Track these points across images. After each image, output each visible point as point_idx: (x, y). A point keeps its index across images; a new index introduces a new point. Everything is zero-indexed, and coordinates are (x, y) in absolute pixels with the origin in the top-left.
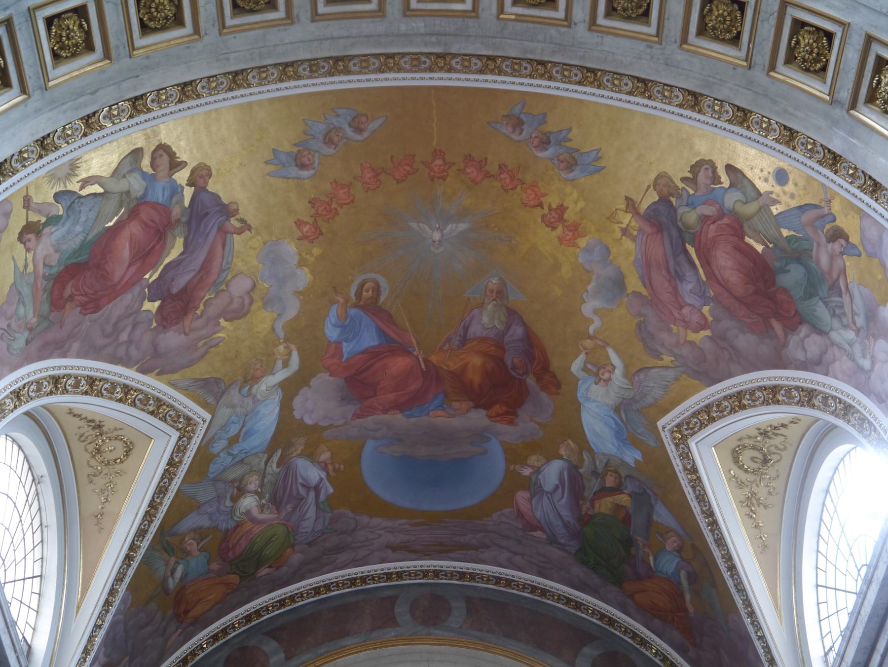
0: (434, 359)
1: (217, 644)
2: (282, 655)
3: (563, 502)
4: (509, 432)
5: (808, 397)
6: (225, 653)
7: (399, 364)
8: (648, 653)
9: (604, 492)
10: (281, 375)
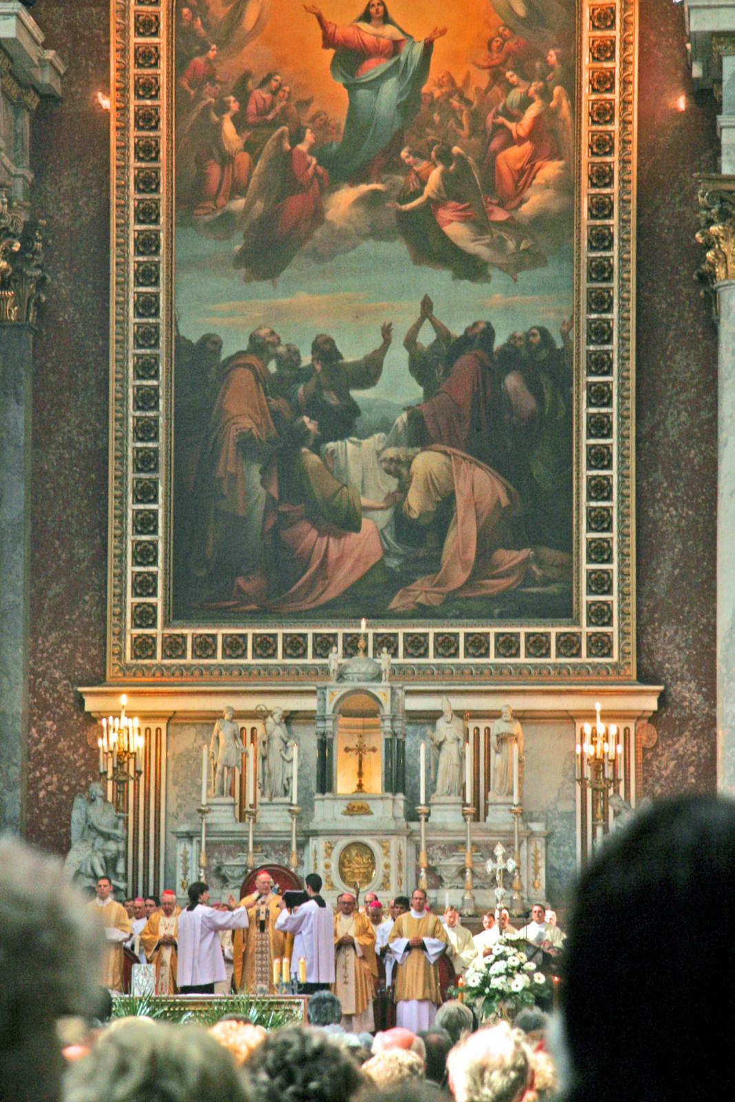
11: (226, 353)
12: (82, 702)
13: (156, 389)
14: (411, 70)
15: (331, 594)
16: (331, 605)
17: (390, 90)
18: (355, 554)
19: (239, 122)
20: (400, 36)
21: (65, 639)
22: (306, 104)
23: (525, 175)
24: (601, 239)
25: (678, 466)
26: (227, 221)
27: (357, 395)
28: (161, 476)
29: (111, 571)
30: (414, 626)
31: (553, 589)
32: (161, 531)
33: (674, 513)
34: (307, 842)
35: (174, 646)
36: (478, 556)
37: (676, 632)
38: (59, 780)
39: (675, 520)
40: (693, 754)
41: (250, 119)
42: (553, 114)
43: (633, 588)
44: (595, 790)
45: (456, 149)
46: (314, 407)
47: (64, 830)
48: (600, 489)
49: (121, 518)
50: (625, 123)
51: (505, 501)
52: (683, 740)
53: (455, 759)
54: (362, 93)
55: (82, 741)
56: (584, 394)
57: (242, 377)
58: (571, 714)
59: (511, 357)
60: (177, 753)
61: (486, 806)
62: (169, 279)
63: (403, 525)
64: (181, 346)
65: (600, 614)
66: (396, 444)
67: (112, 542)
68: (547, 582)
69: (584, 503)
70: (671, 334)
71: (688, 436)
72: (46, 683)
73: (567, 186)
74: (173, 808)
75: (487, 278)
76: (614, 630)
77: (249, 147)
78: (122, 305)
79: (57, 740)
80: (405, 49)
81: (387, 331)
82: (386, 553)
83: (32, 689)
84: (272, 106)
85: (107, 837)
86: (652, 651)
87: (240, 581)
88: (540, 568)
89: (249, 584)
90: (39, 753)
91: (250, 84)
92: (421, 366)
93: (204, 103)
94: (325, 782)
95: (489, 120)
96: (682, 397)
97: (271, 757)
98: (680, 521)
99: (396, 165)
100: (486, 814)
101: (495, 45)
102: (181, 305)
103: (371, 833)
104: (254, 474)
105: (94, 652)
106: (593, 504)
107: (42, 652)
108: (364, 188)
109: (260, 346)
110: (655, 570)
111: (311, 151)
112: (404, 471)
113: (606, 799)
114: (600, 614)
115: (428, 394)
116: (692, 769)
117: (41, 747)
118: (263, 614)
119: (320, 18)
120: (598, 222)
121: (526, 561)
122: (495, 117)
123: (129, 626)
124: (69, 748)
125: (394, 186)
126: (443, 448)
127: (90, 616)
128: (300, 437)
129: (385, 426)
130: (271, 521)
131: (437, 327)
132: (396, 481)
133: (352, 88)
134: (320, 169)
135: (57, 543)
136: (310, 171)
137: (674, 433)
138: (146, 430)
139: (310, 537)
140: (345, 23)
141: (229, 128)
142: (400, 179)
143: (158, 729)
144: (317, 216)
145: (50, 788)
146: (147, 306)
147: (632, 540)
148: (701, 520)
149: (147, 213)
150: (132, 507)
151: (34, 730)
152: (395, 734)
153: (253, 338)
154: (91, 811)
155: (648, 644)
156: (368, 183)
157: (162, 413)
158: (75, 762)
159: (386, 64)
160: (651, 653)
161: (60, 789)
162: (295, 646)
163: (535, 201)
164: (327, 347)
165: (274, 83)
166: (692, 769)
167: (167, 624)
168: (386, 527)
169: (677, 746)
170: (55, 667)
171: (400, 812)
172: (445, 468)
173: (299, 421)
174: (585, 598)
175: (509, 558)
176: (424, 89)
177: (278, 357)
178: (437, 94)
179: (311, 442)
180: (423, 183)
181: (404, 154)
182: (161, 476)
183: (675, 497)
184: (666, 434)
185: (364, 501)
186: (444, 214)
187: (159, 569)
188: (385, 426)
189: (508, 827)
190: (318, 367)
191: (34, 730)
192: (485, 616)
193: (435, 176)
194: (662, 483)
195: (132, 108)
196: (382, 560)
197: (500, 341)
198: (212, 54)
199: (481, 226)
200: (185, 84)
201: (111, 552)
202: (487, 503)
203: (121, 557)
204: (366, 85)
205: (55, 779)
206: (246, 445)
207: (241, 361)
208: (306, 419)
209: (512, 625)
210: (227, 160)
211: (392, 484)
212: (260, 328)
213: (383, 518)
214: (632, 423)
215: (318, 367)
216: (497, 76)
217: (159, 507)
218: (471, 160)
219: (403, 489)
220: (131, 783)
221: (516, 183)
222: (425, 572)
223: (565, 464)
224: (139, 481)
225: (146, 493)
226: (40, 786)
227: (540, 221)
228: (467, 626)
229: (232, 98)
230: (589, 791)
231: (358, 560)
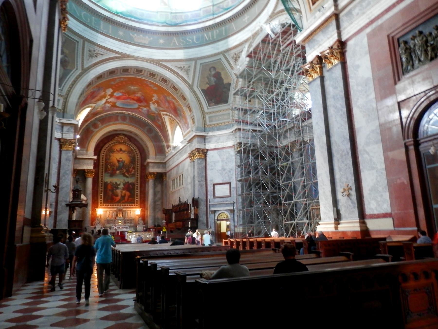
0: (130, 97)
3: (146, 112)
4: (140, 104)
5: (178, 123)
7: (124, 97)
9: (152, 113)
10: (106, 98)
26: (108, 173)
27: (119, 186)
46: (115, 187)
57: (109, 185)
63: (122, 196)
65: (137, 203)
69: (136, 195)
73: (135, 172)
77: (111, 168)
81: (121, 182)
92: (124, 184)
109: (111, 182)
111: (116, 168)
114: (137, 203)
118: (111, 203)
129: (120, 189)
138: (102, 189)
140: (118, 159)
141: (109, 166)
144: (115, 173)
149: (102, 172)
157: (103, 187)
163: (133, 173)
175: (130, 199)
193: (125, 171)
199: (128, 174)
206: (110, 190)
210: (109, 168)
211: (121, 193)
217: (102, 195)
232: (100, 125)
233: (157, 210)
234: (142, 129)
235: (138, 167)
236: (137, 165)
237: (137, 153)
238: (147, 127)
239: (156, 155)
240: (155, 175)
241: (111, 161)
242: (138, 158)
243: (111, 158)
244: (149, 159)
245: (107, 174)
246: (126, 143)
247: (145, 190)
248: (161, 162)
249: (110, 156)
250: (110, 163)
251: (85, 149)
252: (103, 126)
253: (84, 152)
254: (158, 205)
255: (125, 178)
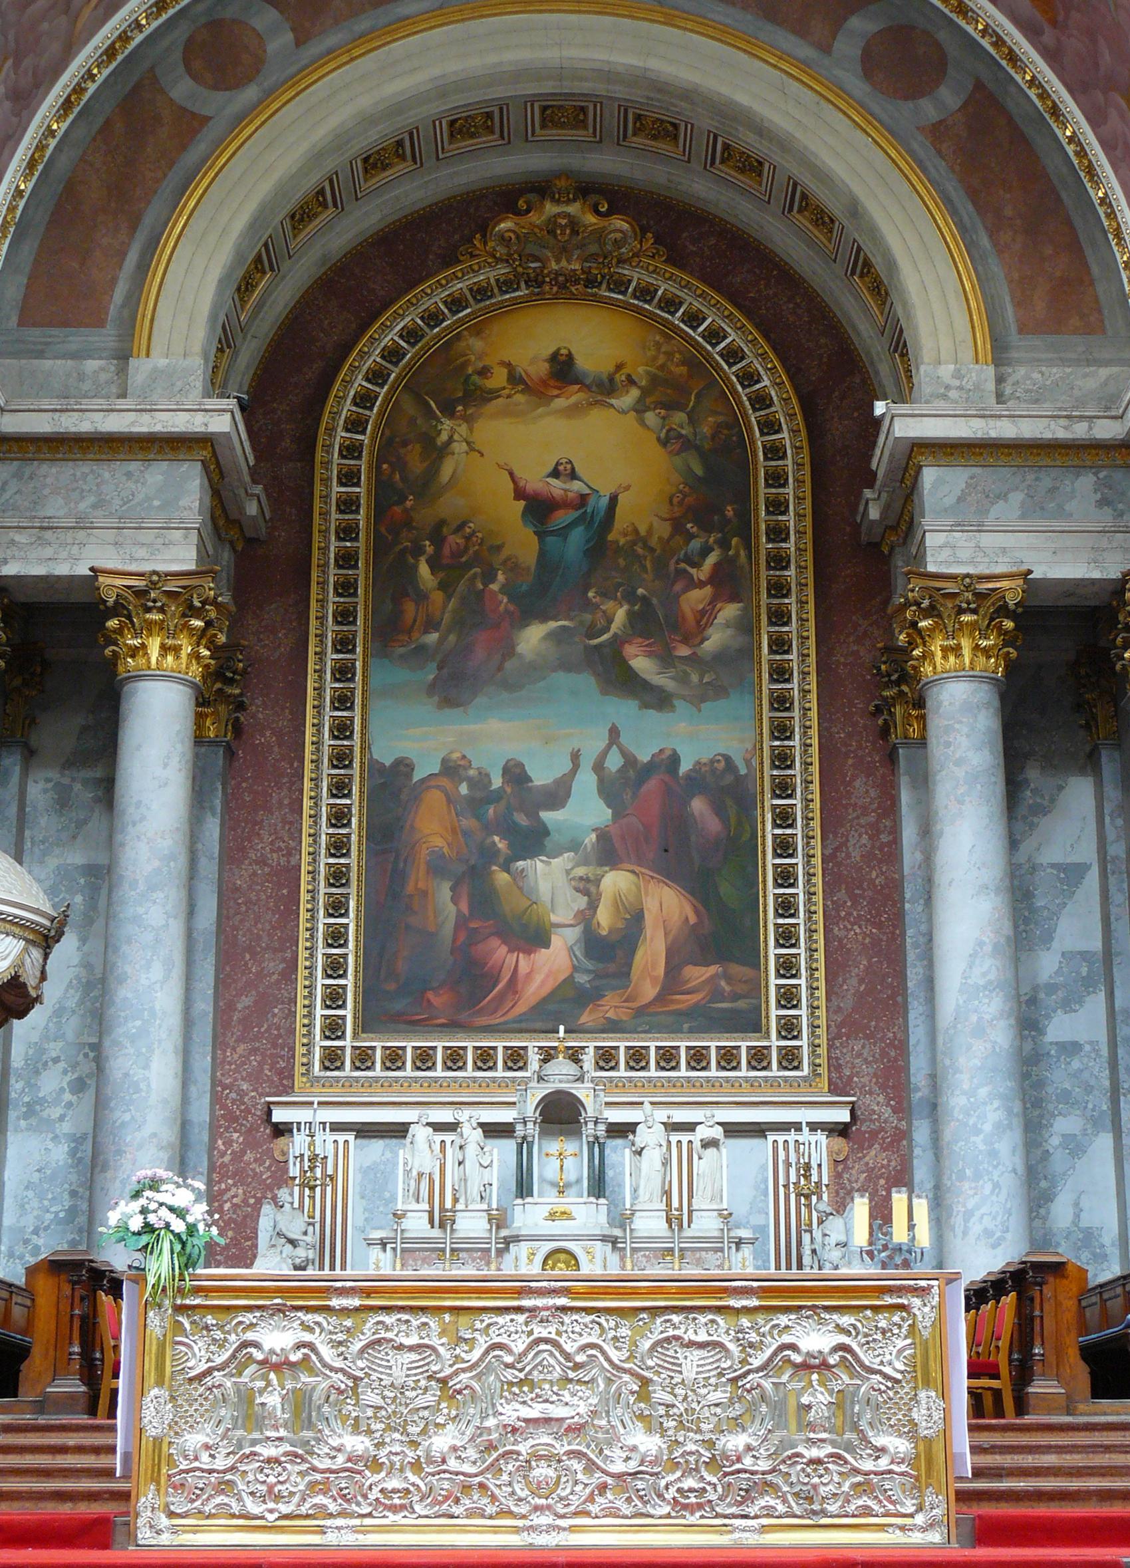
1: (165, 17)
2: (290, 36)
6: (181, 34)
8: (970, 29)
11: (418, 776)
12: (269, 1113)
13: (349, 807)
14: (597, 520)
15: (522, 1008)
16: (520, 1019)
17: (577, 536)
18: (545, 970)
19: (434, 565)
20: (588, 491)
21: (254, 1051)
22: (499, 548)
23: (705, 617)
24: (780, 673)
25: (860, 887)
27: (546, 816)
28: (353, 890)
29: (301, 982)
30: (604, 1040)
31: (741, 1004)
32: (351, 944)
33: (858, 931)
34: (507, 1249)
35: (363, 1058)
36: (667, 973)
37: (863, 1047)
38: (244, 1193)
39: (860, 937)
40: (883, 1166)
41: (445, 561)
42: (732, 561)
43: (823, 1003)
44: (798, 1195)
45: (640, 591)
47: (249, 1243)
48: (786, 907)
49: (312, 930)
50: (801, 569)
51: (693, 919)
52: (873, 1153)
53: (658, 1165)
54: (550, 539)
55: (269, 1153)
56: (769, 816)
57: (435, 798)
58: (764, 1127)
59: (698, 781)
60: (365, 1165)
61: (690, 1212)
62: (364, 706)
64: (374, 769)
66: (585, 862)
67: (302, 954)
68: (735, 997)
70: (850, 762)
71: (868, 857)
72: (233, 1095)
73: (747, 626)
74: (360, 1223)
75: (672, 708)
76: (804, 1042)
77: (444, 586)
78: (318, 727)
79: (243, 1152)
80: (592, 501)
81: (575, 757)
82: (575, 969)
83: (216, 1099)
84: (466, 549)
85: (293, 1243)
86: (840, 1065)
87: (430, 995)
88: (728, 984)
89: (439, 1000)
90: (223, 1165)
91: (445, 530)
92: (608, 790)
93: (401, 547)
94: (524, 1188)
95: (672, 567)
96: (862, 821)
97: (467, 1163)
98: (864, 939)
99: (588, 605)
100: (690, 1222)
101: (675, 500)
102: (373, 727)
103: (576, 1238)
104: (444, 891)
105: (283, 1064)
106: (780, 921)
107: (230, 1064)
108: (553, 625)
109: (451, 770)
110: (841, 986)
111: (504, 589)
112: (593, 889)
113: (809, 1206)
114: (789, 1028)
115: (617, 815)
116: (882, 1182)
117: (227, 1159)
118: (454, 1026)
119: (511, 474)
120: (778, 657)
121: (716, 975)
122: (677, 563)
123: (318, 1038)
124: (256, 1160)
125: (581, 623)
126: (631, 867)
127: (278, 1029)
128: (490, 854)
129: (574, 846)
130: (462, 937)
131: (624, 753)
132: (586, 898)
133: (541, 535)
134: (511, 607)
135: (248, 956)
136: (502, 608)
137: (856, 855)
139: (500, 953)
140: (535, 478)
141: (424, 569)
142: (588, 617)
143: (346, 1141)
145: (235, 1200)
146: (342, 730)
147: (820, 955)
148: (885, 938)
149: (344, 644)
150: (322, 920)
151: (220, 1142)
152: (597, 1138)
153: (444, 761)
154: (279, 1217)
155: (837, 1059)
156: (555, 619)
158: (262, 1173)
159: (574, 515)
160: (839, 1068)
161: (245, 1201)
162: (485, 1058)
164: (518, 771)
165: (468, 530)
166: (882, 1182)
167: (355, 1036)
168: (575, 944)
169: (867, 1159)
170: (243, 1079)
171: (603, 1218)
172: (633, 888)
173: (488, 841)
174: (774, 1012)
175: (697, 974)
176: (610, 537)
177: (470, 780)
178: (622, 541)
179: (501, 860)
180: (610, 621)
181: (591, 594)
182: (353, 890)
183: (859, 916)
184: (848, 856)
185: (554, 918)
186: (629, 650)
187: (349, 982)
188: (574, 846)
189: (716, 1234)
190: (509, 790)
191: (220, 1142)
192: (674, 1030)
193: (620, 615)
194: (845, 902)
195: (332, 549)
196: (571, 976)
197: (685, 767)
198: (409, 504)
199: (666, 659)
200: (383, 530)
201: (302, 963)
202: (675, 919)
203: (311, 968)
204: (552, 533)
205: (240, 1191)
206: (438, 868)
207: (432, 783)
208: (496, 839)
209: (703, 1039)
210: (422, 597)
211: (582, 902)
212: (452, 752)
213: (572, 935)
214: (817, 842)
215: (509, 790)
216: (677, 526)
217: (350, 921)
218: (655, 601)
219: (593, 906)
220: (318, 1189)
221: (698, 622)
222: (614, 989)
223: (750, 883)
224: (331, 895)
225: (337, 907)
226: (225, 1198)
227: (721, 658)
228: (658, 1039)
229: (427, 543)
230: (793, 1196)
231: (548, 976)
232: (280, 42)
233: (1065, 1125)
234: (806, 51)
235: (779, 561)
236: (765, 545)
237: (761, 401)
238: (861, 25)
239: (1000, 354)
240: (1003, 610)
241: (449, 506)
242: (775, 452)
243: (447, 469)
244: (904, 391)
245: (387, 674)
246: (620, 285)
247: (891, 853)
248: (1080, 431)
249: (436, 452)
250: (437, 538)
251: (106, 337)
252: (314, 48)
253: (91, 365)
254: (1071, 1048)
255: (624, 710)
